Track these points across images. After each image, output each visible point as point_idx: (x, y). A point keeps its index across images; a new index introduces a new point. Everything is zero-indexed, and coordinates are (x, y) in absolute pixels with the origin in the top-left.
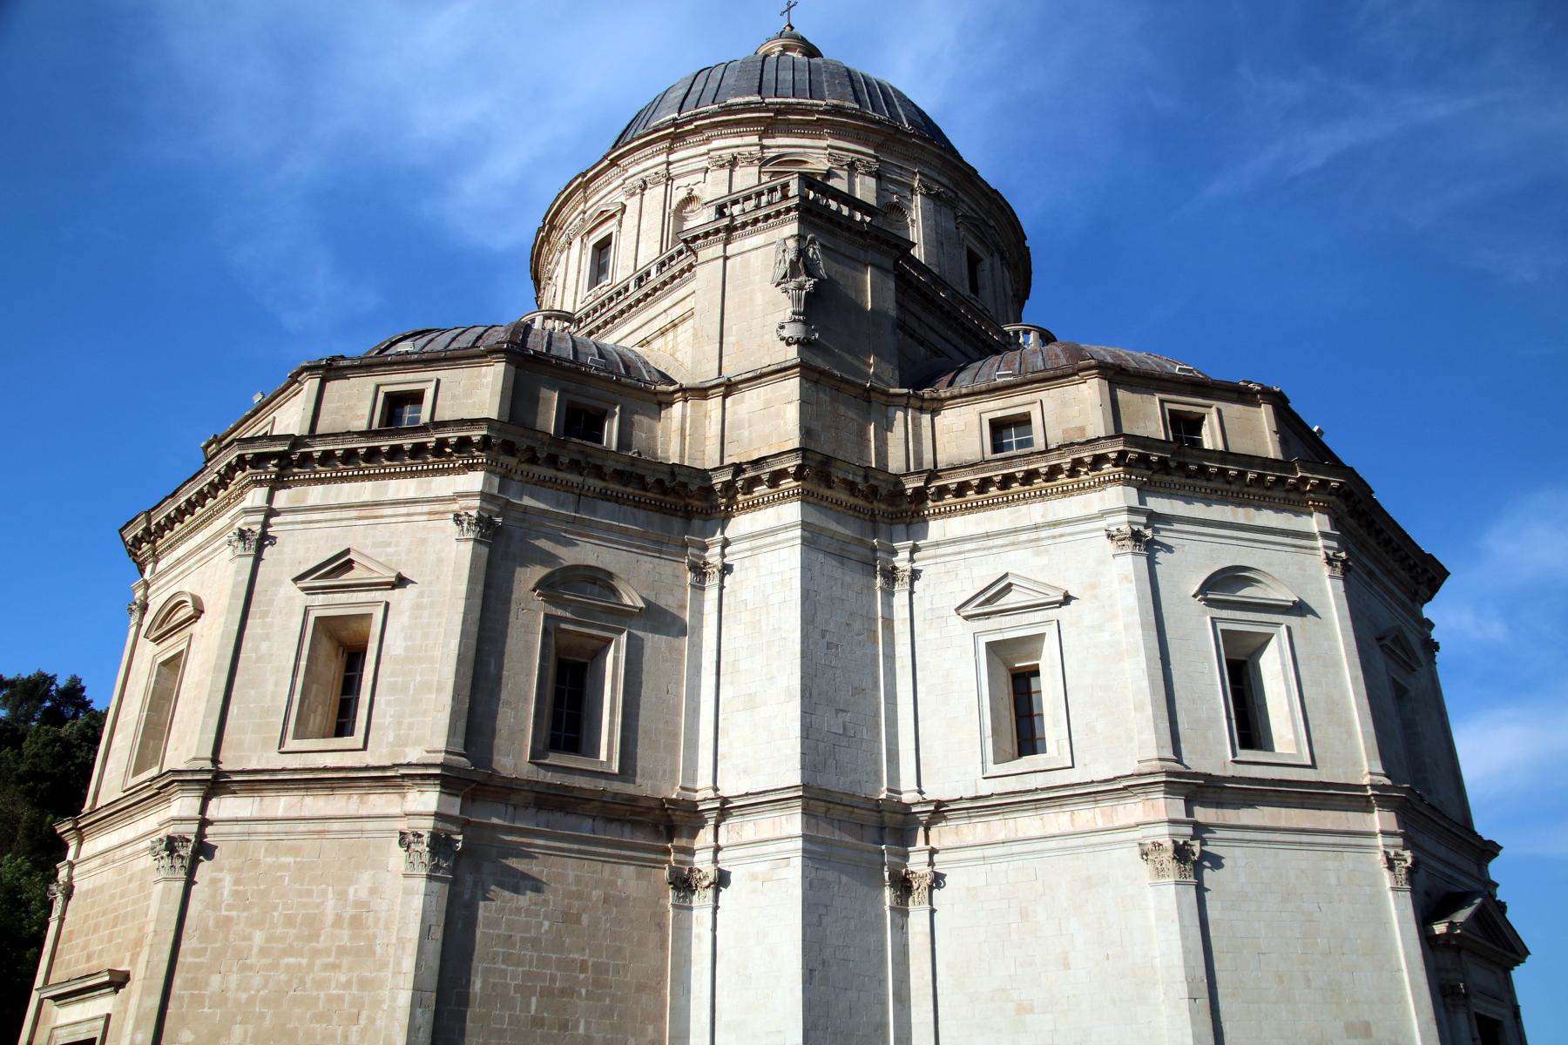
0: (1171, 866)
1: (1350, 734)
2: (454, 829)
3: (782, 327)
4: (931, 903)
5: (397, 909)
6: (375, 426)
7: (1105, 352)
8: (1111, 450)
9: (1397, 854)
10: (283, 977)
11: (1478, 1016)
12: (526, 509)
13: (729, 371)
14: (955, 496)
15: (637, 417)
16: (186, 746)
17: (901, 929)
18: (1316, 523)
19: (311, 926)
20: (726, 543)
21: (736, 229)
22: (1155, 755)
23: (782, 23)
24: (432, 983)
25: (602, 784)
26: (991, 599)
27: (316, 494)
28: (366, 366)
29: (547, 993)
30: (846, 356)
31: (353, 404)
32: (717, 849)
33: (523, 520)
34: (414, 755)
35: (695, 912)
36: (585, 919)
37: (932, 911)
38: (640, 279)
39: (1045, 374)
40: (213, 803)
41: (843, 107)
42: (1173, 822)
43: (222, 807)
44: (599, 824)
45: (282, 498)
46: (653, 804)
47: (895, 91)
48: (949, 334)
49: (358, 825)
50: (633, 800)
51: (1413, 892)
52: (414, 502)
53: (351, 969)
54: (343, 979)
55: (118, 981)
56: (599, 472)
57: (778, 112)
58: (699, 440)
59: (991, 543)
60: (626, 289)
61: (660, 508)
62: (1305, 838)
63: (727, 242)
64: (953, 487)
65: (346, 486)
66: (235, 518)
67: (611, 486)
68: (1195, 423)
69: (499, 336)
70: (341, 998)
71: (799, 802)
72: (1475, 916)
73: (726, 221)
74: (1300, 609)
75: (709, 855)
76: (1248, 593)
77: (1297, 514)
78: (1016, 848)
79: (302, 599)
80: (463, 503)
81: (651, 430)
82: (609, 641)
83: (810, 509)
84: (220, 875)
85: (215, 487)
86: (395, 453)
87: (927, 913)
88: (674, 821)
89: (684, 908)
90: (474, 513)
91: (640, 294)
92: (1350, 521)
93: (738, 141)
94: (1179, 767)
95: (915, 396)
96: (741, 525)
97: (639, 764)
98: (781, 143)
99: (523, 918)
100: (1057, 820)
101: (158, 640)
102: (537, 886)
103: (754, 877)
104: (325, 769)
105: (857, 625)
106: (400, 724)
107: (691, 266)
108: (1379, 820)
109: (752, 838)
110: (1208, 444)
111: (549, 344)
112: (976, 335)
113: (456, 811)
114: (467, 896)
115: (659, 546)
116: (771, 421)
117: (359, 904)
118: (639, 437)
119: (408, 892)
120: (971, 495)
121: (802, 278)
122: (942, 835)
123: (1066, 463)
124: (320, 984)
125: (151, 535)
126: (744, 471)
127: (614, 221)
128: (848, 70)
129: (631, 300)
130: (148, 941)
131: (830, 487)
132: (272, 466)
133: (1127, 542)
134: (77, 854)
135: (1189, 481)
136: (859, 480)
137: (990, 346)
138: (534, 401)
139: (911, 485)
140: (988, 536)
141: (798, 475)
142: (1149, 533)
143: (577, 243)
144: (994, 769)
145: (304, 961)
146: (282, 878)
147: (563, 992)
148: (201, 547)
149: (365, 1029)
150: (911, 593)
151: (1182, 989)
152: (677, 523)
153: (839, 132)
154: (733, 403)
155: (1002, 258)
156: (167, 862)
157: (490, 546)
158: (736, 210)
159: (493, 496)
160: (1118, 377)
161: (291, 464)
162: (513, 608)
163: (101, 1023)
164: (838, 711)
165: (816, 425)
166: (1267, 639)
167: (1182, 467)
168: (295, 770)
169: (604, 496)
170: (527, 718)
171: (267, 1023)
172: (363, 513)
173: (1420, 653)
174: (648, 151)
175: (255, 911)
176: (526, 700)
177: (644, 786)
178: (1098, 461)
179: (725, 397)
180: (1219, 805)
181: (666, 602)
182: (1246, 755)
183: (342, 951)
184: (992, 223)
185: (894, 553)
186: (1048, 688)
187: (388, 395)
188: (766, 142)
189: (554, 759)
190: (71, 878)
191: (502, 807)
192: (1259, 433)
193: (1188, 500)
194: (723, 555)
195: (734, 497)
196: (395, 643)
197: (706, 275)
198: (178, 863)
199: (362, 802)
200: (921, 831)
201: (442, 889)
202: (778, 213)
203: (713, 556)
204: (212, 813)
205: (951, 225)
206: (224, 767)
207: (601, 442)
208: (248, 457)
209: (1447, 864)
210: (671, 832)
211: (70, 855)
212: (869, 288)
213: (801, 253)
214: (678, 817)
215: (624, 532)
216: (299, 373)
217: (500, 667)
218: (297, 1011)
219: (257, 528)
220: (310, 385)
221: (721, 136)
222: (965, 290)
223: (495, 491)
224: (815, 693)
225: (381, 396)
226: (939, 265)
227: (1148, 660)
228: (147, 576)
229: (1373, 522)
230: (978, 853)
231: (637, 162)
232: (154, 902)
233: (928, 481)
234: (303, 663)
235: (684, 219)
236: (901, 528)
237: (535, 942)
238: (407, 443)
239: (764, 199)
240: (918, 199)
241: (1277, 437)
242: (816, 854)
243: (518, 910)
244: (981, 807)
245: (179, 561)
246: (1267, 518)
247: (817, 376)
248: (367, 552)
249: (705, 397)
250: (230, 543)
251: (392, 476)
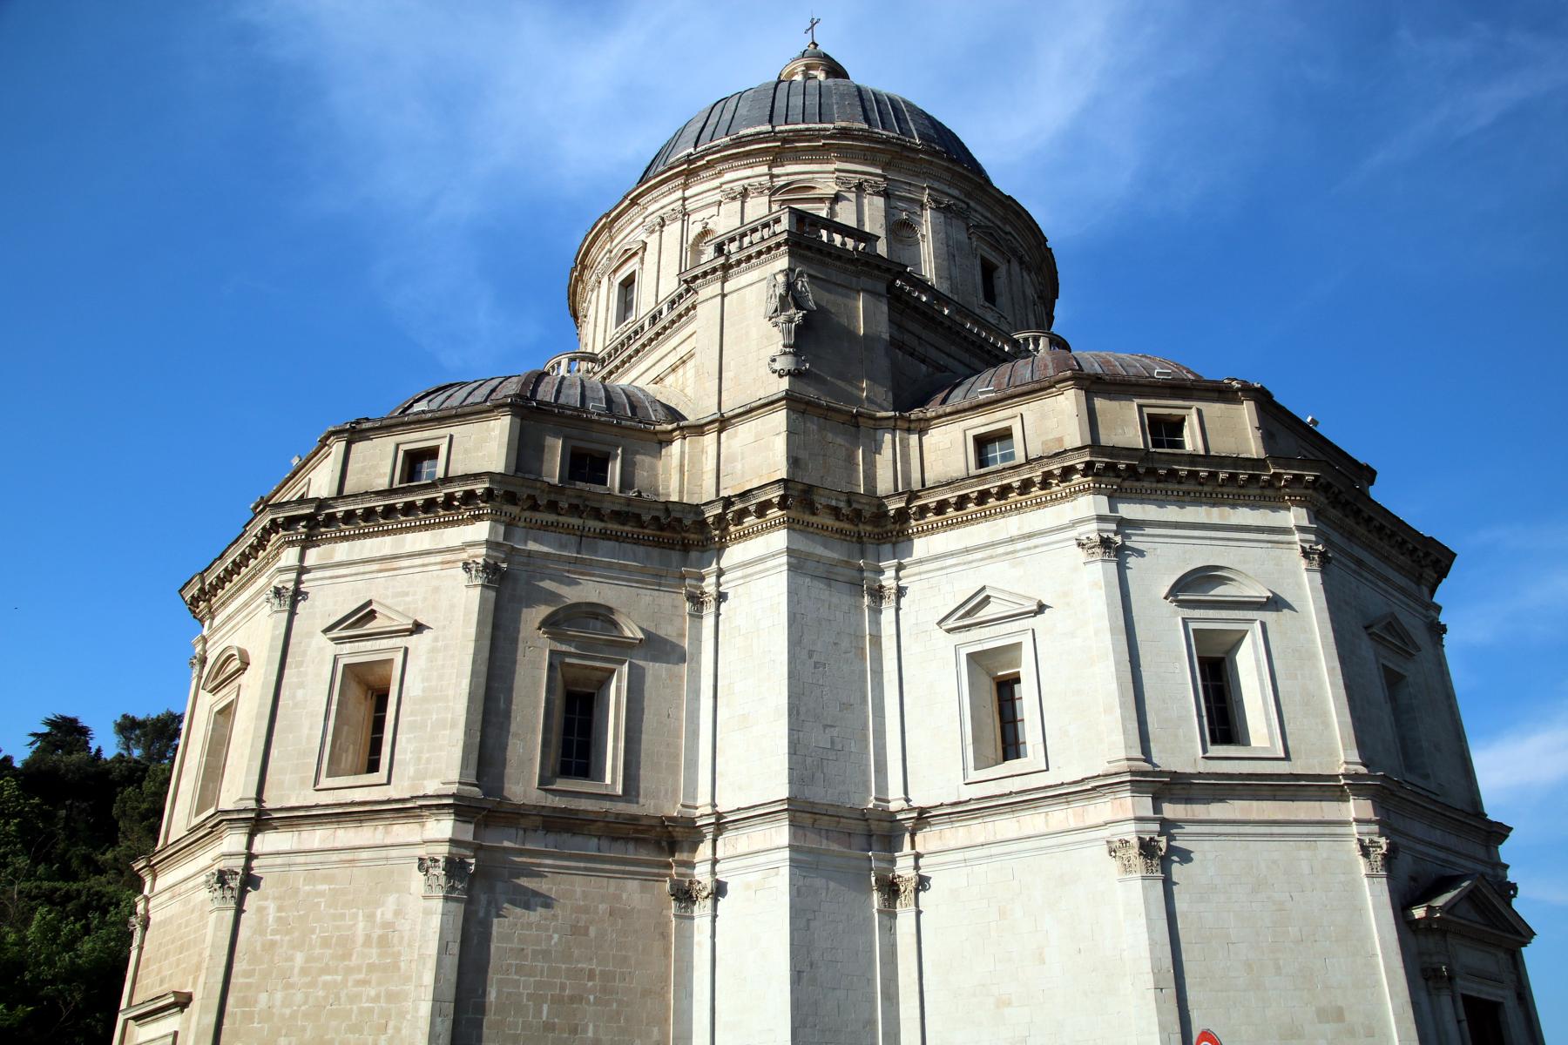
0: (1138, 862)
1: (1327, 725)
2: (468, 853)
3: (774, 360)
4: (917, 905)
5: (418, 927)
6: (396, 485)
7: (1090, 358)
8: (1079, 461)
9: (1371, 841)
10: (321, 993)
11: (1465, 998)
12: (530, 554)
14: (937, 514)
15: (638, 458)
16: (235, 791)
17: (889, 930)
18: (1294, 516)
19: (344, 946)
20: (720, 573)
21: (731, 266)
22: (1123, 755)
23: (804, 43)
24: (450, 993)
25: (607, 805)
26: (972, 610)
27: (342, 551)
28: (386, 428)
29: (557, 1000)
30: (839, 383)
31: (376, 463)
32: (715, 862)
33: (528, 564)
34: (432, 787)
35: (696, 921)
36: (592, 931)
37: (919, 913)
38: (654, 318)
39: (1030, 387)
40: (258, 838)
41: (850, 129)
42: (1139, 820)
43: (266, 842)
44: (605, 843)
45: (313, 556)
46: (653, 822)
47: (909, 105)
48: (953, 349)
49: (383, 853)
50: (634, 819)
51: (1388, 877)
52: (428, 553)
53: (379, 984)
54: (373, 993)
55: (182, 1002)
56: (597, 514)
57: (784, 141)
58: (698, 475)
59: (970, 557)
60: (642, 328)
61: (658, 544)
62: (1276, 830)
63: (724, 280)
65: (368, 542)
66: (272, 577)
67: (610, 526)
68: (1177, 425)
69: (512, 388)
70: (371, 1010)
71: (786, 815)
72: (1471, 896)
73: (722, 260)
74: (1275, 603)
75: (707, 867)
76: (1221, 592)
77: (1274, 509)
78: (995, 850)
79: (332, 649)
80: (472, 551)
81: (653, 468)
82: (612, 672)
83: (796, 535)
84: (265, 903)
86: (409, 509)
87: (913, 914)
88: (673, 837)
89: (686, 917)
90: (480, 561)
91: (651, 334)
92: (1334, 513)
93: (748, 172)
94: (1147, 767)
95: (902, 417)
96: (734, 554)
97: (642, 785)
98: (790, 171)
99: (534, 932)
100: (1032, 821)
101: (214, 690)
102: (547, 902)
103: (748, 886)
104: (353, 804)
105: (845, 644)
106: (419, 759)
107: (694, 307)
108: (1355, 808)
109: (747, 850)
110: (1189, 447)
111: (559, 392)
112: (981, 347)
113: (469, 837)
114: (481, 914)
115: (657, 579)
116: (760, 453)
117: (388, 925)
118: (641, 477)
119: (428, 912)
120: (951, 512)
121: (792, 311)
122: (927, 840)
123: (1037, 475)
124: (353, 999)
125: (206, 594)
126: (733, 504)
127: (636, 259)
128: (859, 89)
129: (644, 340)
130: (205, 965)
131: (814, 514)
132: (301, 528)
133: (1097, 550)
134: (152, 889)
135: (1161, 485)
136: (842, 505)
137: (997, 356)
138: (540, 449)
139: (894, 506)
140: (967, 551)
141: (782, 504)
142: (1118, 539)
143: (605, 280)
144: (974, 775)
145: (339, 978)
146: (318, 904)
147: (572, 999)
148: (246, 604)
149: (391, 1039)
150: (898, 609)
151: (1148, 980)
152: (675, 556)
153: (846, 154)
155: (1021, 262)
156: (219, 893)
157: (497, 591)
158: (734, 247)
159: (498, 544)
160: (1095, 386)
161: (318, 524)
162: (521, 646)
164: (825, 726)
165: (803, 455)
166: (1242, 635)
167: (1151, 472)
168: (327, 806)
169: (605, 535)
170: (534, 749)
171: (308, 1035)
172: (384, 566)
173: (1420, 635)
174: (664, 188)
175: (296, 934)
176: (534, 731)
177: (649, 805)
178: (1067, 473)
179: (720, 432)
180: (1188, 800)
181: (666, 631)
183: (372, 968)
184: (1008, 228)
185: (881, 572)
186: (1026, 692)
187: (407, 453)
188: (776, 171)
189: (562, 784)
191: (513, 831)
192: (1238, 431)
193: (1161, 504)
194: (718, 585)
195: (726, 528)
197: (707, 312)
198: (228, 894)
199: (387, 833)
200: (907, 837)
201: (458, 909)
202: (769, 249)
203: (709, 585)
205: (963, 237)
206: (267, 805)
207: (605, 483)
208: (280, 521)
209: (1448, 849)
210: (673, 847)
211: (146, 892)
212: (862, 313)
213: (790, 286)
214: (678, 832)
215: (624, 568)
216: (327, 438)
217: (509, 702)
218: (333, 1023)
219: (291, 586)
220: (338, 448)
221: (732, 169)
222: (977, 301)
223: (500, 539)
224: (803, 710)
225: (401, 454)
226: (950, 278)
227: (1117, 663)
228: (205, 632)
229: (1359, 511)
230: (959, 856)
231: (655, 200)
232: (210, 930)
233: (909, 502)
234: (334, 707)
235: (702, 253)
236: (887, 548)
237: (546, 954)
238: (419, 499)
239: (746, 240)
240: (928, 214)
241: (1259, 434)
242: (803, 862)
243: (530, 925)
244: (961, 811)
245: (230, 618)
247: (803, 406)
248: (388, 602)
249: (702, 434)
250: (268, 600)
251: (408, 530)
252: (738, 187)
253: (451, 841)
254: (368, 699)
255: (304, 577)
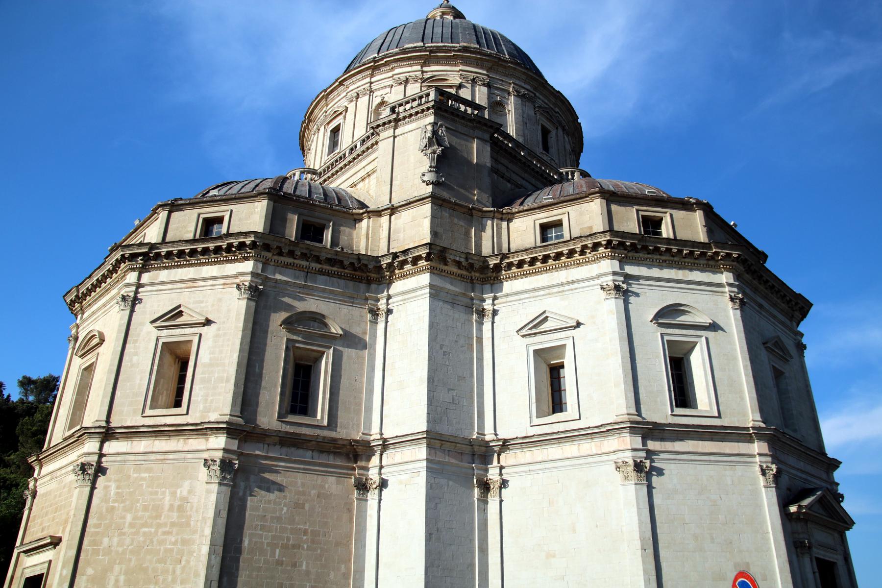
0: (633, 475)
1: (742, 398)
2: (234, 457)
3: (424, 175)
4: (500, 496)
5: (203, 501)
6: (197, 237)
7: (609, 184)
8: (603, 240)
9: (767, 467)
10: (141, 539)
11: (817, 559)
12: (277, 281)
13: (395, 202)
14: (518, 268)
15: (342, 228)
16: (93, 416)
17: (484, 511)
18: (725, 277)
19: (157, 510)
20: (389, 297)
21: (400, 120)
22: (625, 412)
24: (221, 541)
25: (317, 432)
26: (537, 325)
27: (164, 275)
28: (193, 204)
29: (285, 547)
30: (462, 190)
31: (186, 225)
32: (381, 467)
33: (275, 287)
34: (213, 417)
35: (369, 502)
36: (307, 506)
37: (501, 501)
38: (352, 149)
39: (574, 197)
40: (106, 444)
41: (469, 47)
42: (634, 450)
43: (111, 447)
44: (316, 454)
45: (146, 278)
46: (345, 442)
47: (502, 36)
48: (526, 175)
49: (183, 456)
50: (334, 440)
51: (777, 488)
52: (216, 278)
53: (177, 534)
54: (173, 539)
55: (55, 542)
56: (318, 260)
57: (431, 52)
58: (377, 240)
59: (537, 294)
60: (345, 155)
61: (352, 279)
62: (712, 458)
63: (395, 128)
64: (516, 263)
65: (180, 270)
66: (121, 289)
67: (325, 267)
68: (658, 223)
69: (268, 184)
70: (172, 550)
71: (425, 441)
72: (820, 501)
73: (394, 116)
74: (714, 327)
75: (377, 470)
76: (683, 319)
77: (714, 273)
78: (548, 465)
79: (156, 333)
80: (242, 278)
81: (350, 235)
82: (323, 353)
83: (435, 277)
84: (109, 484)
85: (110, 272)
86: (205, 251)
87: (498, 502)
88: (356, 452)
89: (363, 500)
90: (247, 284)
91: (350, 158)
92: (747, 277)
93: (409, 69)
94: (638, 419)
95: (498, 211)
96: (397, 287)
97: (339, 421)
98: (433, 69)
99: (272, 506)
100: (570, 449)
101: (82, 356)
102: (281, 488)
104: (165, 425)
105: (462, 341)
106: (206, 400)
107: (377, 143)
108: (758, 447)
109: (401, 461)
110: (664, 235)
111: (296, 188)
112: (542, 175)
113: (235, 448)
114: (241, 494)
115: (351, 300)
116: (415, 228)
117: (184, 499)
118: (343, 239)
119: (208, 492)
120: (526, 267)
121: (436, 147)
122: (507, 458)
123: (578, 247)
124: (161, 543)
125: (79, 299)
126: (398, 257)
127: (341, 117)
128: (474, 26)
129: (346, 162)
130: (70, 520)
131: (446, 264)
132: (139, 260)
133: (612, 292)
134: (39, 474)
135: (649, 256)
136: (462, 260)
137: (550, 181)
138: (284, 220)
139: (492, 262)
140: (535, 290)
141: (428, 258)
142: (625, 286)
143: (322, 129)
144: (536, 421)
145: (153, 530)
146: (142, 485)
147: (294, 546)
148: (104, 305)
149: (184, 567)
150: (493, 323)
151: (638, 544)
152: (363, 286)
153: (466, 61)
154: (395, 218)
155: (564, 130)
156: (81, 477)
157: (257, 302)
158: (401, 109)
159: (258, 275)
160: (612, 197)
161: (150, 259)
162: (269, 335)
163: (47, 565)
164: (449, 390)
165: (440, 230)
166: (694, 345)
167: (645, 248)
168: (149, 426)
169: (321, 272)
170: (276, 396)
171: (133, 564)
172: (189, 285)
173: (793, 350)
174: (359, 76)
175: (128, 503)
176: (276, 386)
177: (342, 433)
178: (596, 246)
179: (391, 215)
180: (662, 439)
181: (356, 330)
182: (678, 411)
183: (173, 524)
184: (557, 110)
185: (484, 300)
186: (568, 373)
187: (204, 219)
188: (425, 69)
189: (291, 418)
190: (35, 487)
191: (261, 445)
192: (693, 227)
193: (650, 267)
194: (388, 304)
195: (393, 271)
196: (204, 356)
197: (384, 146)
198: (87, 477)
199: (185, 443)
200: (496, 456)
201: (227, 490)
202: (423, 111)
204: (105, 450)
205: (532, 113)
206: (112, 425)
207: (321, 241)
208: (127, 255)
209: (807, 473)
210: (356, 458)
211: (36, 475)
212: (475, 151)
213: (435, 132)
214: (360, 449)
215: (332, 292)
216: (157, 209)
217: (262, 368)
218: (148, 557)
219: (132, 295)
220: (163, 215)
221: (399, 67)
222: (539, 150)
223: (260, 272)
224: (436, 379)
225: (201, 220)
226: (524, 136)
227: (623, 358)
228: (78, 321)
229: (762, 276)
230: (526, 468)
231: (354, 83)
232: (74, 499)
233: (502, 260)
234: (155, 368)
235: (380, 114)
236: (488, 286)
237: (279, 519)
238: (212, 246)
240: (512, 98)
241: (705, 229)
242: (434, 469)
243: (269, 502)
244: (528, 442)
245: (94, 313)
246: (696, 276)
247: (441, 202)
248: (191, 306)
249: (380, 216)
251: (204, 264)
252: (403, 77)
253: (224, 450)
254: (176, 363)
255: (140, 290)
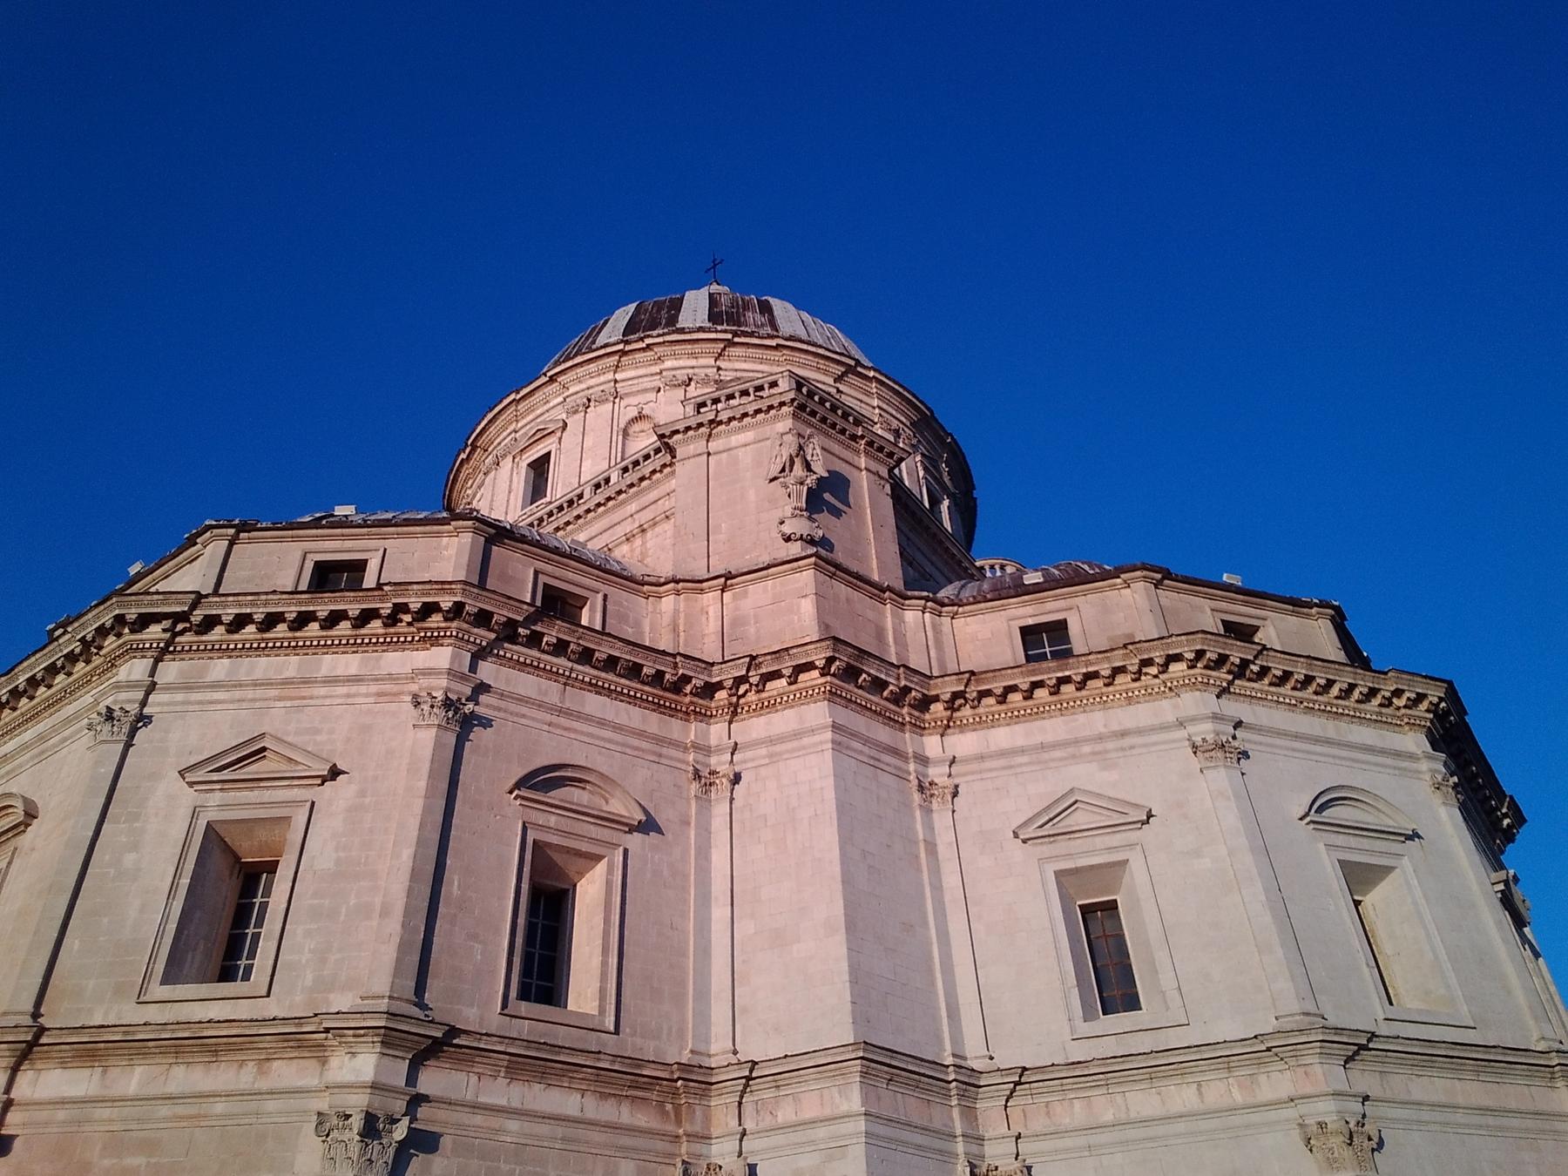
26: (1049, 825)
34: (343, 1001)
42: (1337, 1094)
45: (170, 670)
79: (189, 796)
80: (424, 682)
93: (693, 362)
107: (672, 464)
129: (580, 510)
143: (507, 463)
154: (735, 598)
172: (286, 693)
196: (322, 853)
199: (261, 1072)
219: (133, 708)
221: (674, 356)
223: (466, 671)
225: (309, 566)
250: (90, 727)
252: (682, 375)
253: (375, 1087)
